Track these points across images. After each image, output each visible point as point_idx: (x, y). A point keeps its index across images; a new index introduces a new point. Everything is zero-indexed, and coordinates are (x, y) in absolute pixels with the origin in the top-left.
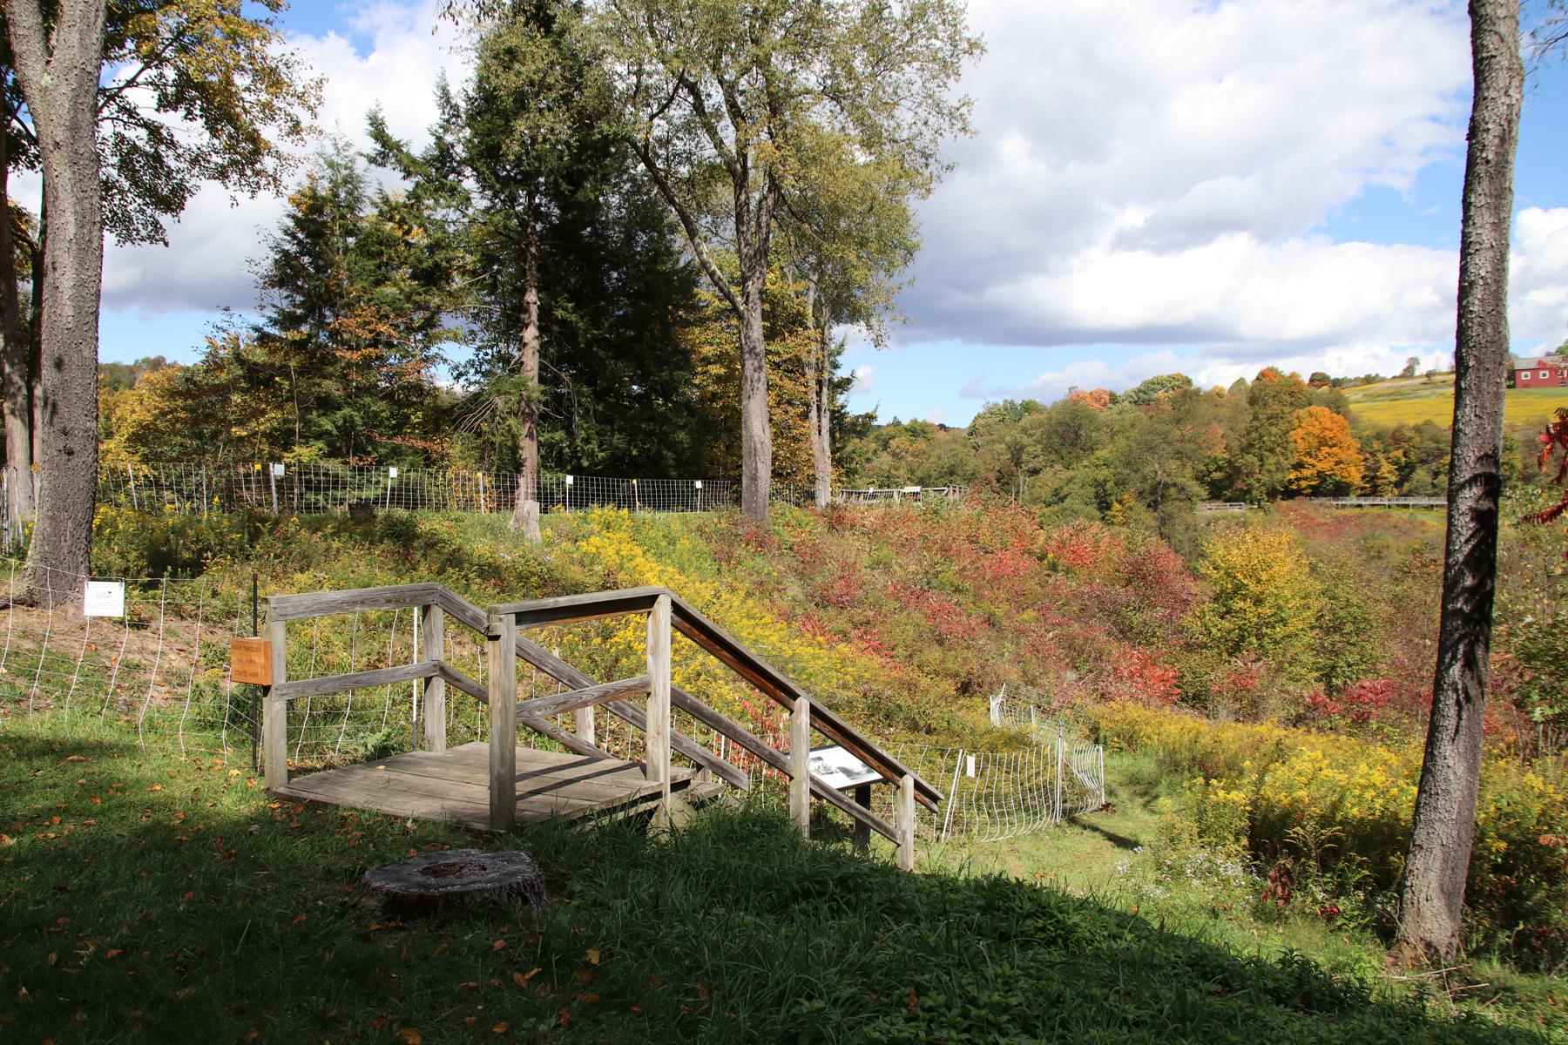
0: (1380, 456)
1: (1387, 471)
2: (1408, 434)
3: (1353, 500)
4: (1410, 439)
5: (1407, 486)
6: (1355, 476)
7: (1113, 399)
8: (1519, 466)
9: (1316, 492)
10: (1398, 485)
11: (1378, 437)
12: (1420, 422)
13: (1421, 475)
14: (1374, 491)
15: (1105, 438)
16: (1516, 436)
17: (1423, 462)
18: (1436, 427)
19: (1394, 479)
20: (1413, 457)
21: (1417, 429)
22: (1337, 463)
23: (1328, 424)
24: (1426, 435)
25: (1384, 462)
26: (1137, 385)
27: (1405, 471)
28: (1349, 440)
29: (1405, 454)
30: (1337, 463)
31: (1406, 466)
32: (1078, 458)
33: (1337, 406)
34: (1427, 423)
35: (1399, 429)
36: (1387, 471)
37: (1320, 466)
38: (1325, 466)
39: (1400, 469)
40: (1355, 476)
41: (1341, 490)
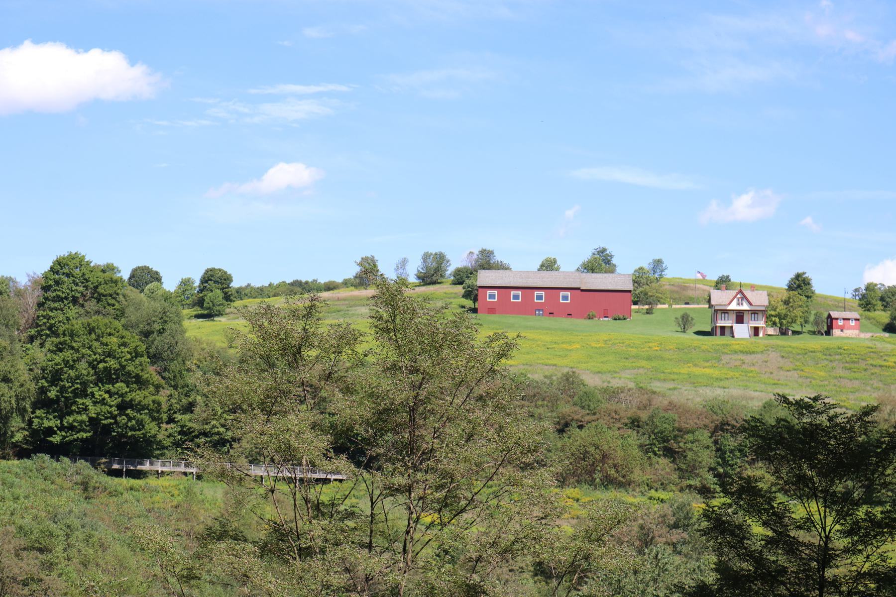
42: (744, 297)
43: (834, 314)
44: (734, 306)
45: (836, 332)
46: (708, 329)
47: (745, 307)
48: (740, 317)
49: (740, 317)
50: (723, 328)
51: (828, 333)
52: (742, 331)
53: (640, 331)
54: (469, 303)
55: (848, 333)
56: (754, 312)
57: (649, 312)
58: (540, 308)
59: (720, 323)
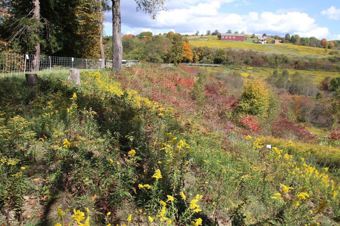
0: (195, 54)
1: (197, 57)
2: (202, 49)
3: (190, 64)
4: (202, 50)
5: (201, 61)
6: (191, 58)
7: (133, 37)
8: (226, 58)
9: (183, 62)
10: (199, 60)
11: (195, 49)
12: (204, 46)
13: (205, 58)
14: (194, 62)
15: (135, 46)
16: (225, 51)
17: (205, 55)
18: (208, 48)
19: (198, 59)
20: (203, 54)
21: (204, 48)
22: (187, 55)
23: (186, 46)
24: (206, 49)
25: (196, 55)
26: (139, 34)
27: (201, 58)
28: (190, 50)
29: (201, 54)
30: (187, 55)
31: (201, 56)
32: (129, 51)
33: (187, 41)
34: (206, 47)
35: (200, 48)
36: (197, 57)
37: (184, 56)
38: (185, 56)
39: (200, 57)
40: (191, 58)
41: (188, 61)
42: (263, 38)
43: (275, 40)
44: (261, 39)
45: (275, 43)
46: (257, 42)
47: (263, 39)
48: (262, 41)
49: (262, 41)
50: (260, 42)
51: (274, 43)
52: (263, 43)
53: (244, 42)
54: (218, 38)
55: (277, 43)
56: (265, 40)
57: (246, 40)
58: (230, 39)
59: (259, 42)
